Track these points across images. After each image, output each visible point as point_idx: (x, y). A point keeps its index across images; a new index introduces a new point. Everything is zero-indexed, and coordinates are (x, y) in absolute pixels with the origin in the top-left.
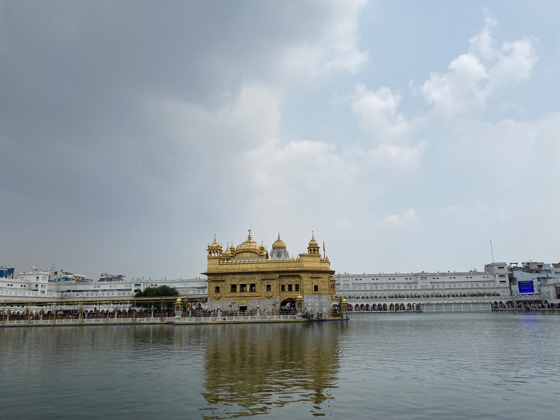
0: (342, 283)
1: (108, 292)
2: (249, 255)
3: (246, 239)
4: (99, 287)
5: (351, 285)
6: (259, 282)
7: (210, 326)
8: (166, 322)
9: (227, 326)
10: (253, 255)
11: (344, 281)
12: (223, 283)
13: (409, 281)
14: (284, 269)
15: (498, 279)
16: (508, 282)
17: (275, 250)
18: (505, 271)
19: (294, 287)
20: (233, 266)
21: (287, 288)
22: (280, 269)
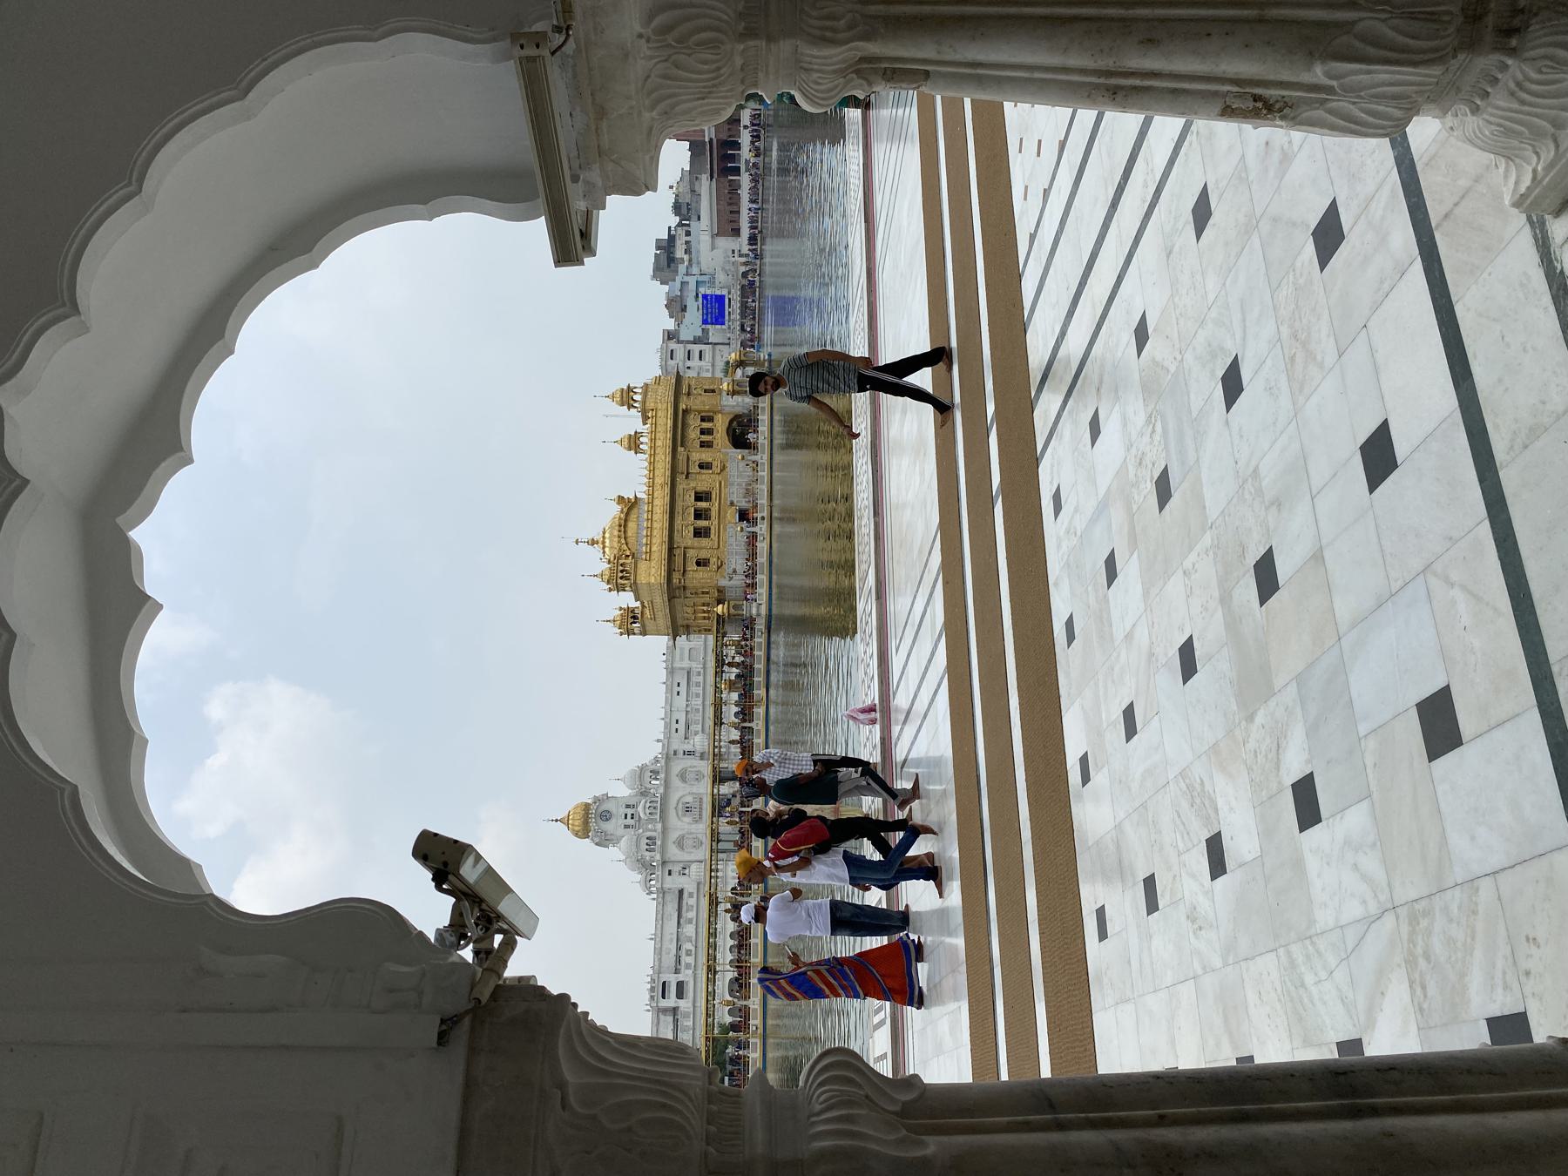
0: (686, 664)
2: (632, 525)
3: (598, 547)
8: (763, 692)
9: (775, 514)
10: (633, 516)
11: (682, 659)
12: (691, 553)
14: (669, 435)
15: (695, 362)
16: (703, 347)
17: (592, 825)
18: (680, 351)
19: (705, 425)
21: (705, 438)
22: (669, 442)
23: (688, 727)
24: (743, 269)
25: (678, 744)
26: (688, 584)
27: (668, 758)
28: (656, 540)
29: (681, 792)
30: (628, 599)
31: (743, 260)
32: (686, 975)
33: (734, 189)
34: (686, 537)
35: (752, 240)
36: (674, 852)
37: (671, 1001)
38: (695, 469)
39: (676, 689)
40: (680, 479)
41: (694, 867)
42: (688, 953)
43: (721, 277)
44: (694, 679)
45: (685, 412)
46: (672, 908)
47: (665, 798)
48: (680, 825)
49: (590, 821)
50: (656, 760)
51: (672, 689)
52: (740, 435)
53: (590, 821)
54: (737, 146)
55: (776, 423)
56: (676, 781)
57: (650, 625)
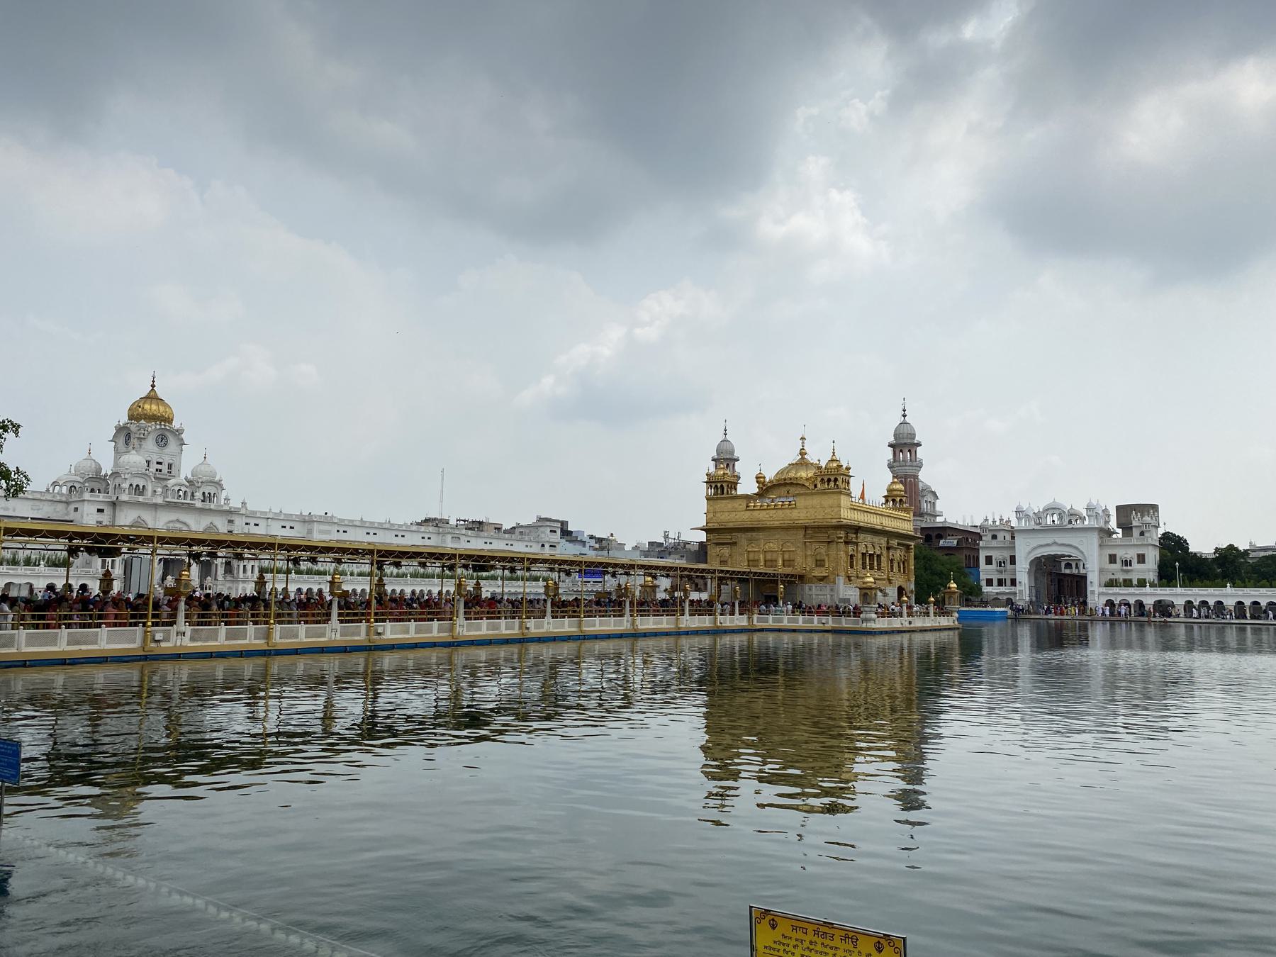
6: (885, 552)
11: (321, 532)
13: (427, 542)
17: (152, 426)
26: (834, 546)
27: (230, 512)
30: (748, 486)
34: (862, 549)
39: (288, 525)
45: (908, 547)
47: (189, 508)
49: (149, 421)
51: (287, 520)
53: (149, 421)
55: (937, 634)
57: (722, 505)
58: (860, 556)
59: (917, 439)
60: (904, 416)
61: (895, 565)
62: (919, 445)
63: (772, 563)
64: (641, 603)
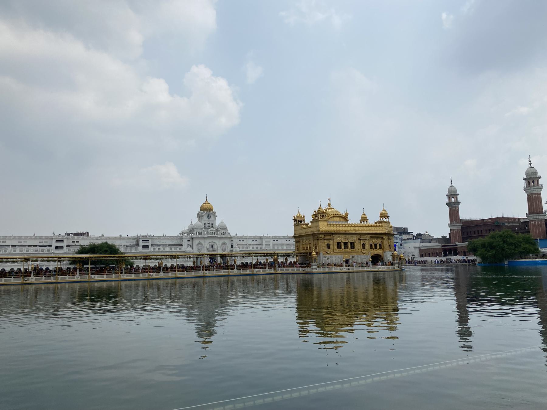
0: (264, 243)
1: (21, 248)
2: (338, 219)
4: (5, 242)
5: (271, 245)
7: (339, 275)
8: (280, 272)
9: (351, 274)
10: (341, 219)
11: (266, 242)
12: (331, 241)
14: (374, 232)
17: (205, 212)
19: (378, 246)
20: (338, 228)
21: (373, 245)
22: (371, 232)
23: (241, 245)
24: (407, 259)
25: (235, 241)
26: (319, 241)
27: (230, 238)
28: (335, 228)
29: (218, 244)
30: (308, 220)
31: (410, 259)
32: (151, 249)
33: (440, 255)
35: (420, 262)
36: (196, 242)
37: (141, 244)
38: (362, 242)
40: (358, 236)
41: (191, 249)
42: (159, 249)
43: (403, 251)
44: (259, 246)
45: (382, 238)
46: (175, 242)
47: (216, 237)
48: (206, 244)
49: (207, 211)
50: (229, 234)
51: (255, 238)
52: (376, 259)
53: (207, 211)
54: (456, 255)
56: (222, 241)
58: (336, 244)
59: (539, 175)
60: (530, 164)
61: (367, 246)
62: (540, 178)
63: (307, 249)
64: (206, 267)
